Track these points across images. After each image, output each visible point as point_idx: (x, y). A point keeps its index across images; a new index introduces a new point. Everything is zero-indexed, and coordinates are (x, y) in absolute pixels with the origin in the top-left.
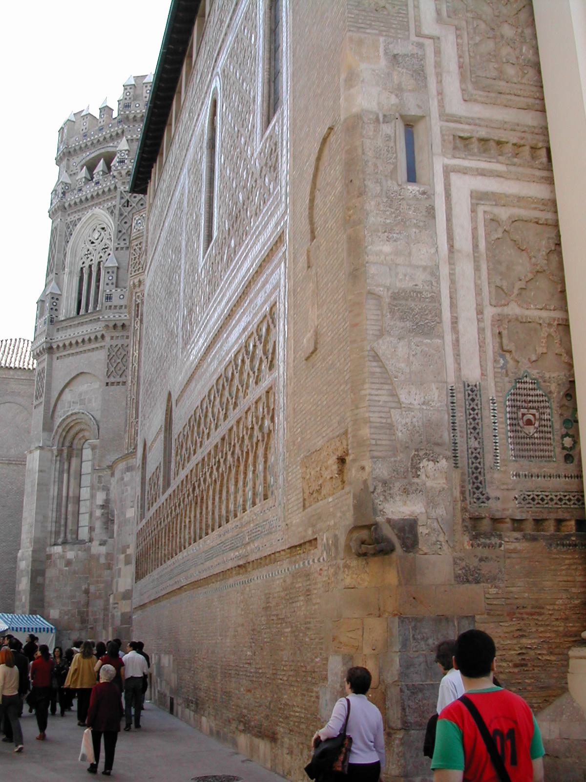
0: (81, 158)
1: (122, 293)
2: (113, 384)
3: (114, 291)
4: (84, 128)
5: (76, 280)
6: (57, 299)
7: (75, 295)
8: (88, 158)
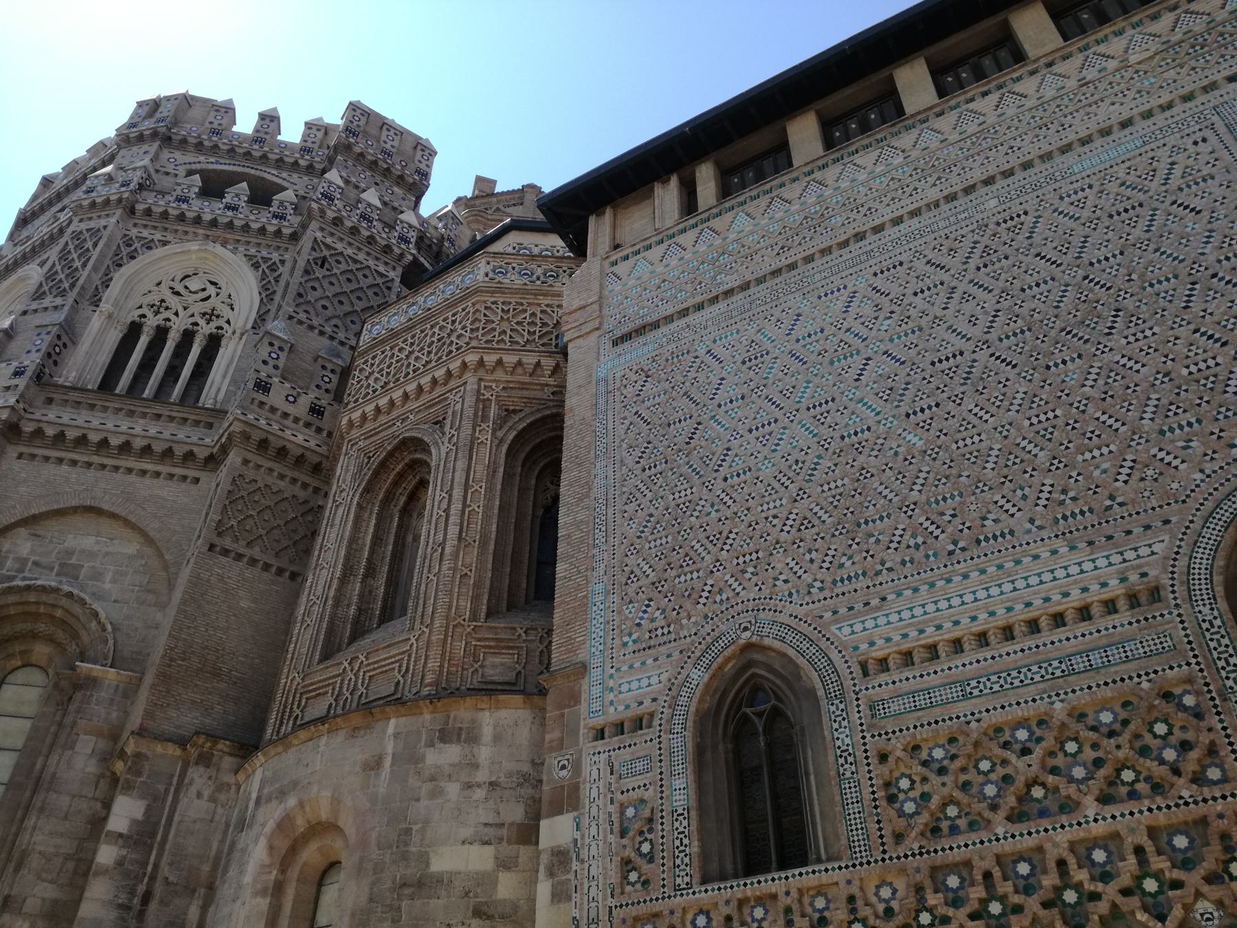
0: (189, 158)
1: (295, 393)
2: (225, 552)
3: (276, 380)
4: (216, 123)
5: (113, 337)
6: (65, 345)
7: (104, 358)
8: (211, 167)
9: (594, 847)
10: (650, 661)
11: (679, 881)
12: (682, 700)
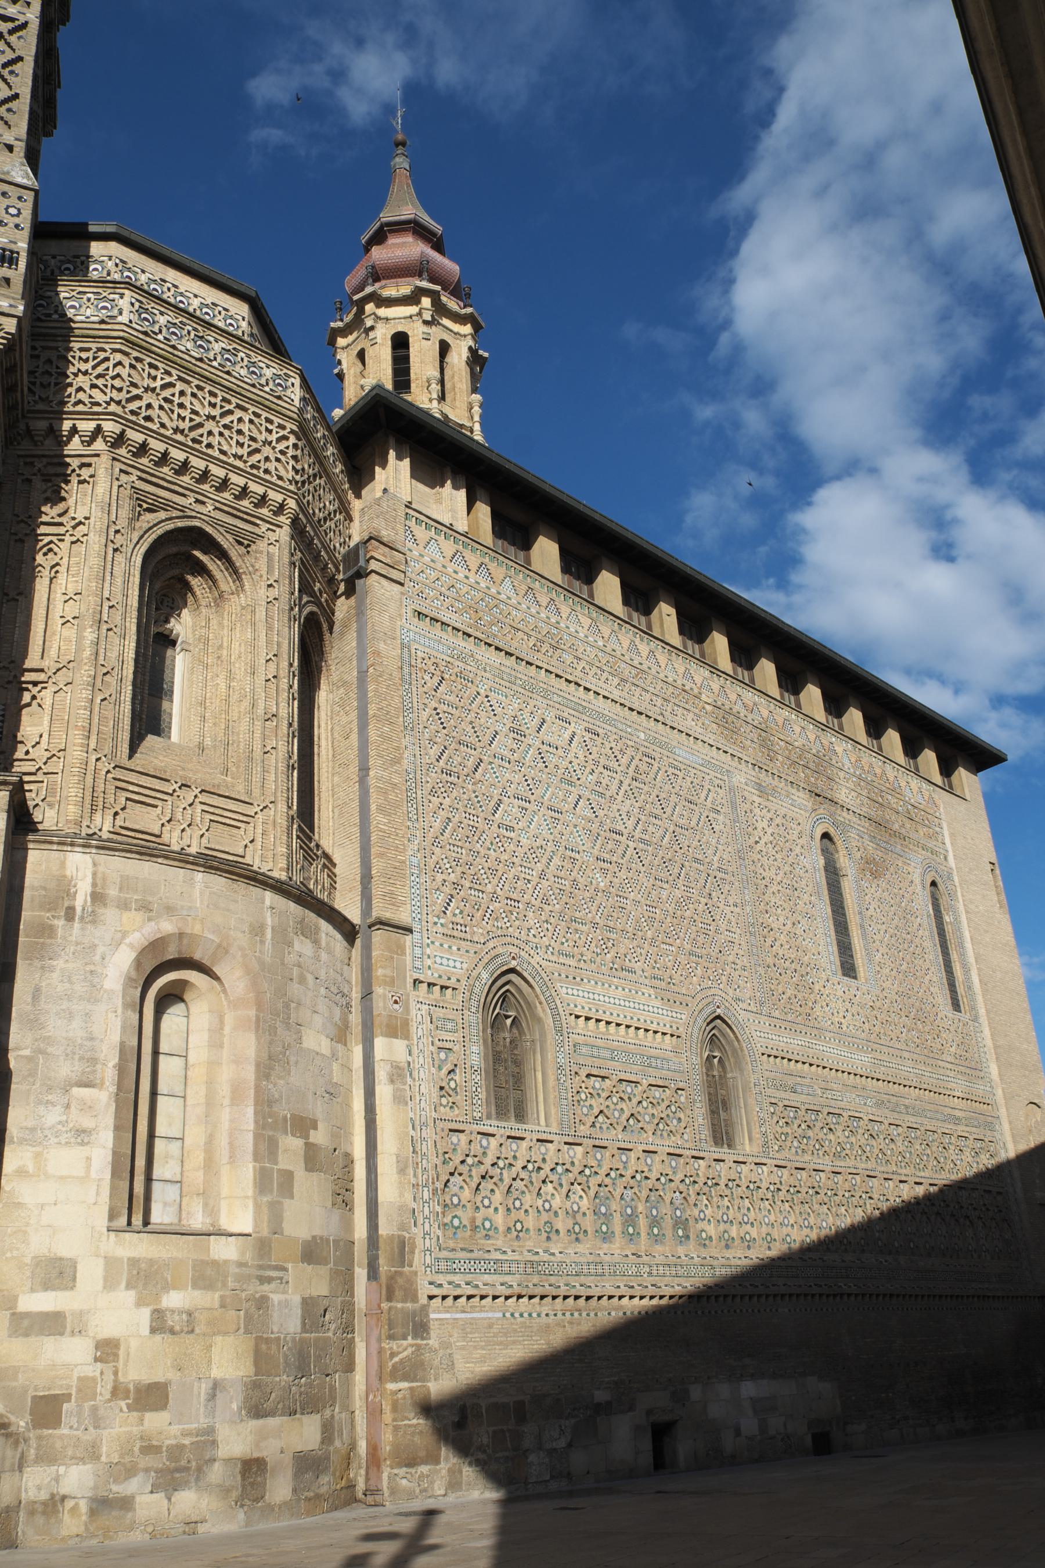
9: (421, 1072)
10: (454, 948)
11: (475, 1114)
12: (476, 990)
